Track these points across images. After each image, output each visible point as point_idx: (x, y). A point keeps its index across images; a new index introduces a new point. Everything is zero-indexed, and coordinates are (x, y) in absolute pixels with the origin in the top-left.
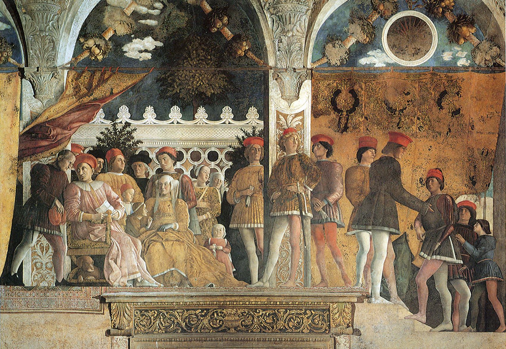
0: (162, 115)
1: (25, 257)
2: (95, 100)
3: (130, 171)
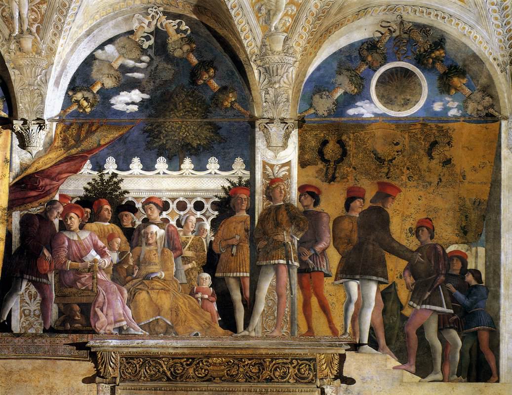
0: (148, 166)
2: (83, 151)
3: (116, 220)
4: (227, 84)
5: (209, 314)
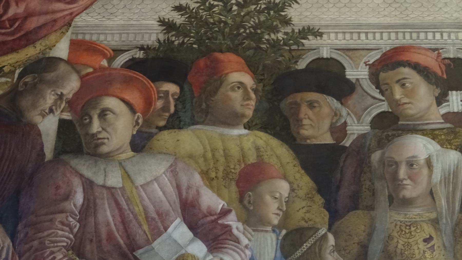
3: (275, 120)
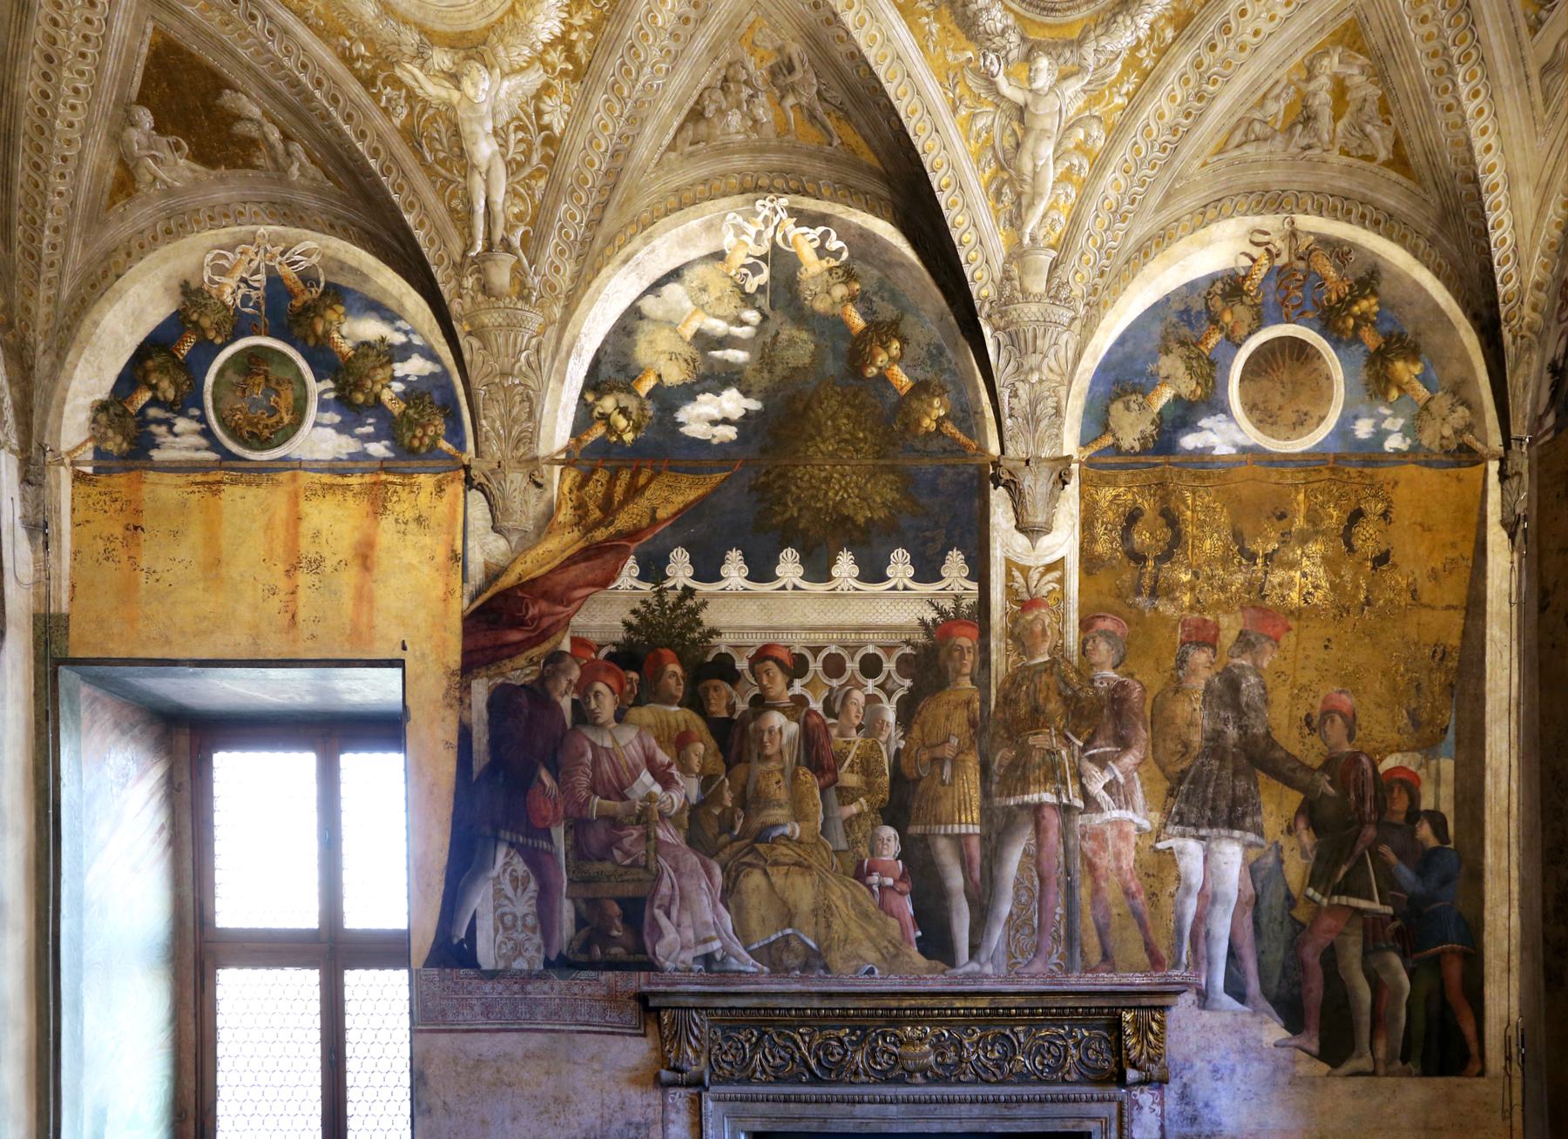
1: (481, 900)
2: (620, 535)
3: (695, 701)
4: (929, 376)
5: (894, 922)
